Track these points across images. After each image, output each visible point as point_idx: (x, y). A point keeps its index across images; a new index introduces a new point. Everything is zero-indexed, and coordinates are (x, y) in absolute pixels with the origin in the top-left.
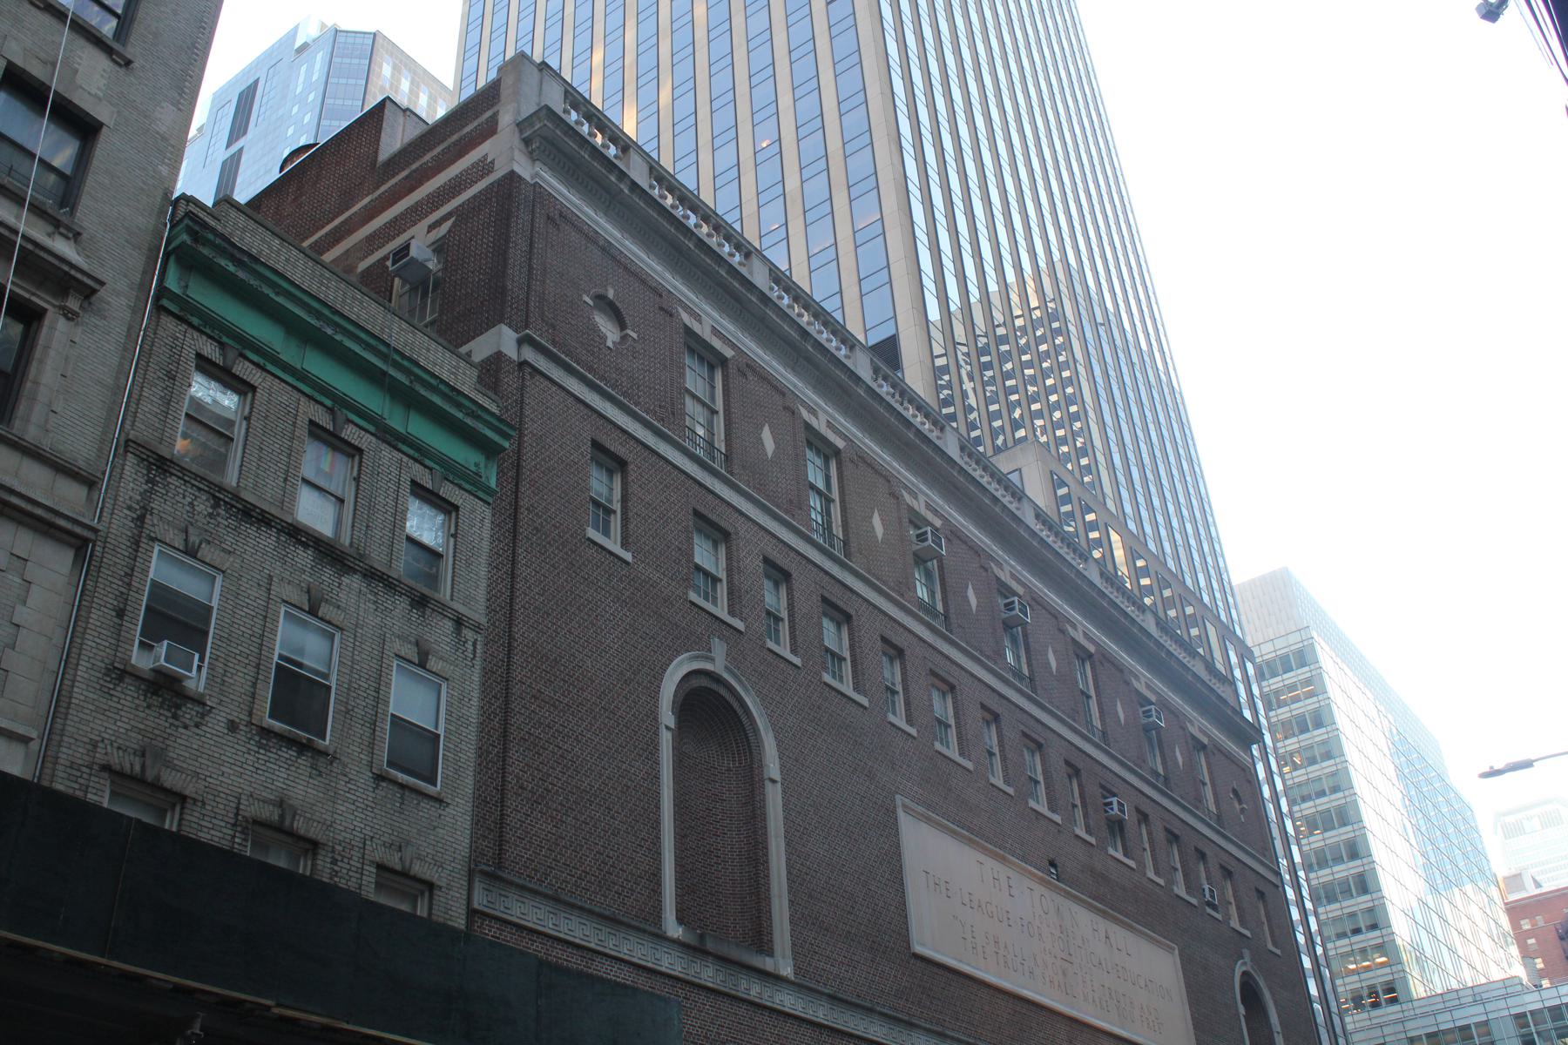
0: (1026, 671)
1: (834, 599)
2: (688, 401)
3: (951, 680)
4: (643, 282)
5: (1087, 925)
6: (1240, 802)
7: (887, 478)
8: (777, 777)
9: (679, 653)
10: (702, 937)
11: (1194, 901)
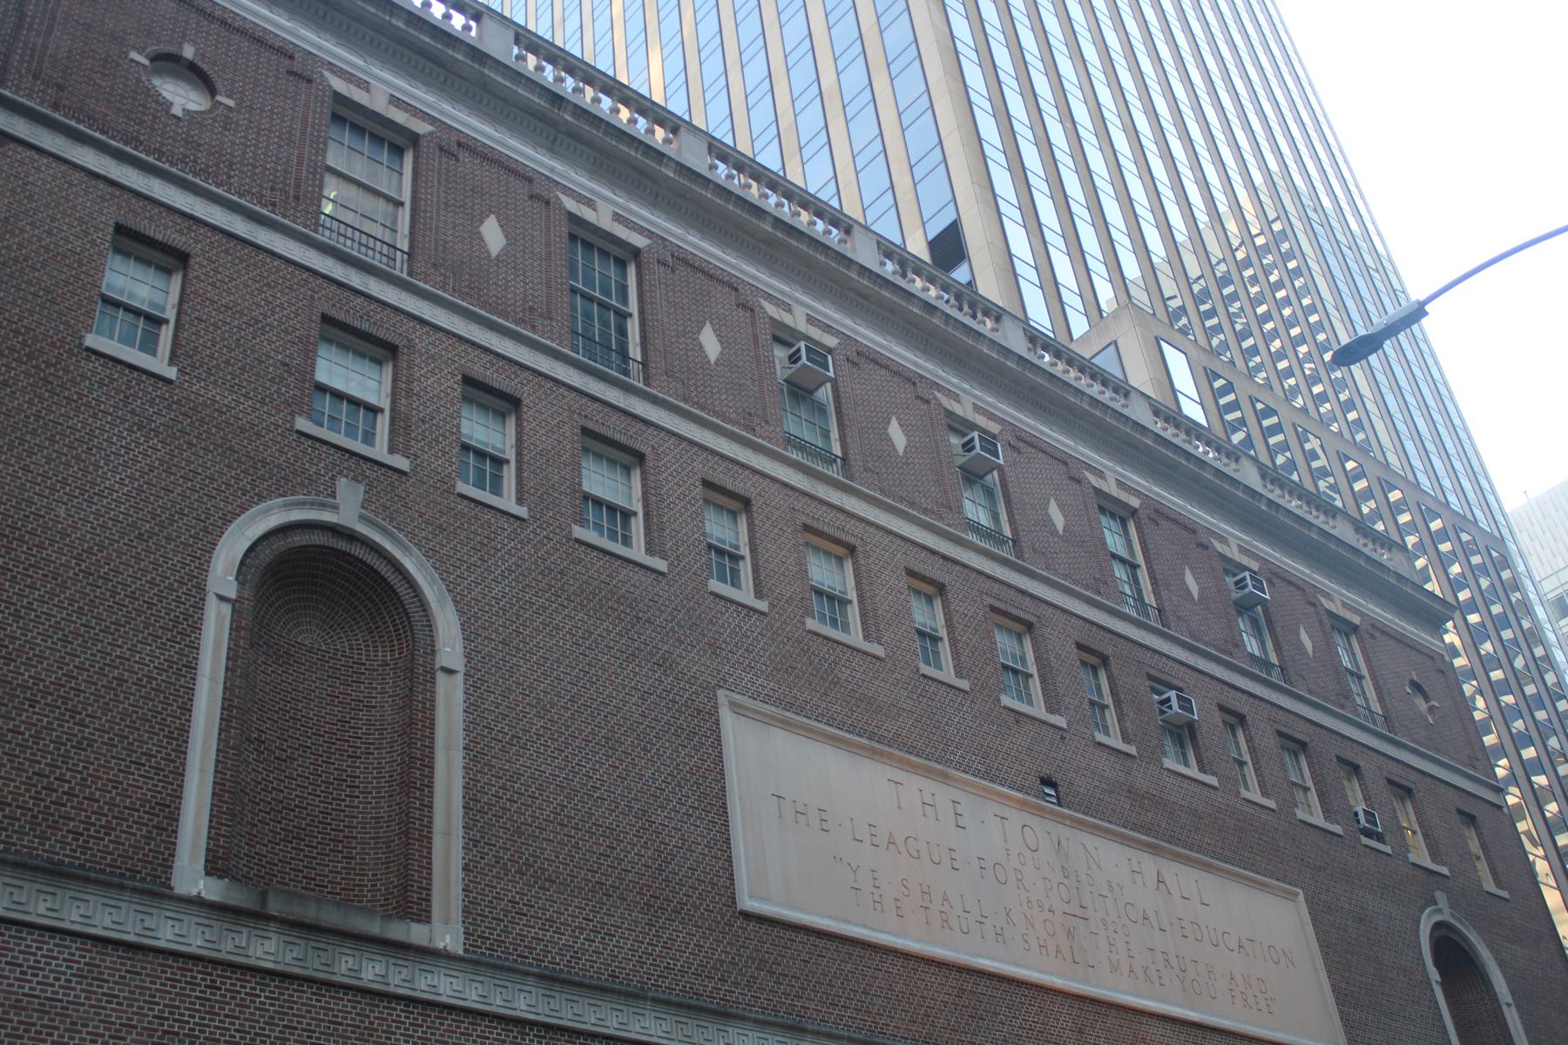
0: (1008, 532)
3: (852, 540)
5: (1116, 865)
6: (1427, 698)
7: (732, 285)
8: (458, 663)
10: (264, 896)
11: (1337, 829)
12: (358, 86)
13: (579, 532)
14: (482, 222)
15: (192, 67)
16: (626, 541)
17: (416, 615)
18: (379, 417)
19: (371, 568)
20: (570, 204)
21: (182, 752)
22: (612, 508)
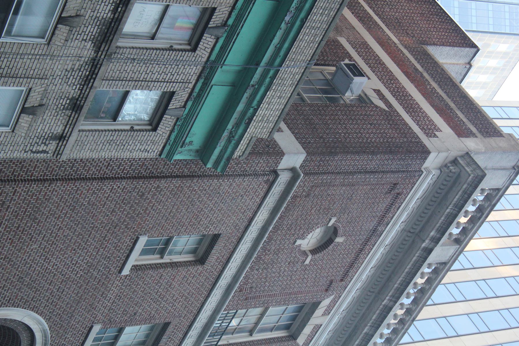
2: (258, 311)
4: (351, 265)
9: (48, 320)
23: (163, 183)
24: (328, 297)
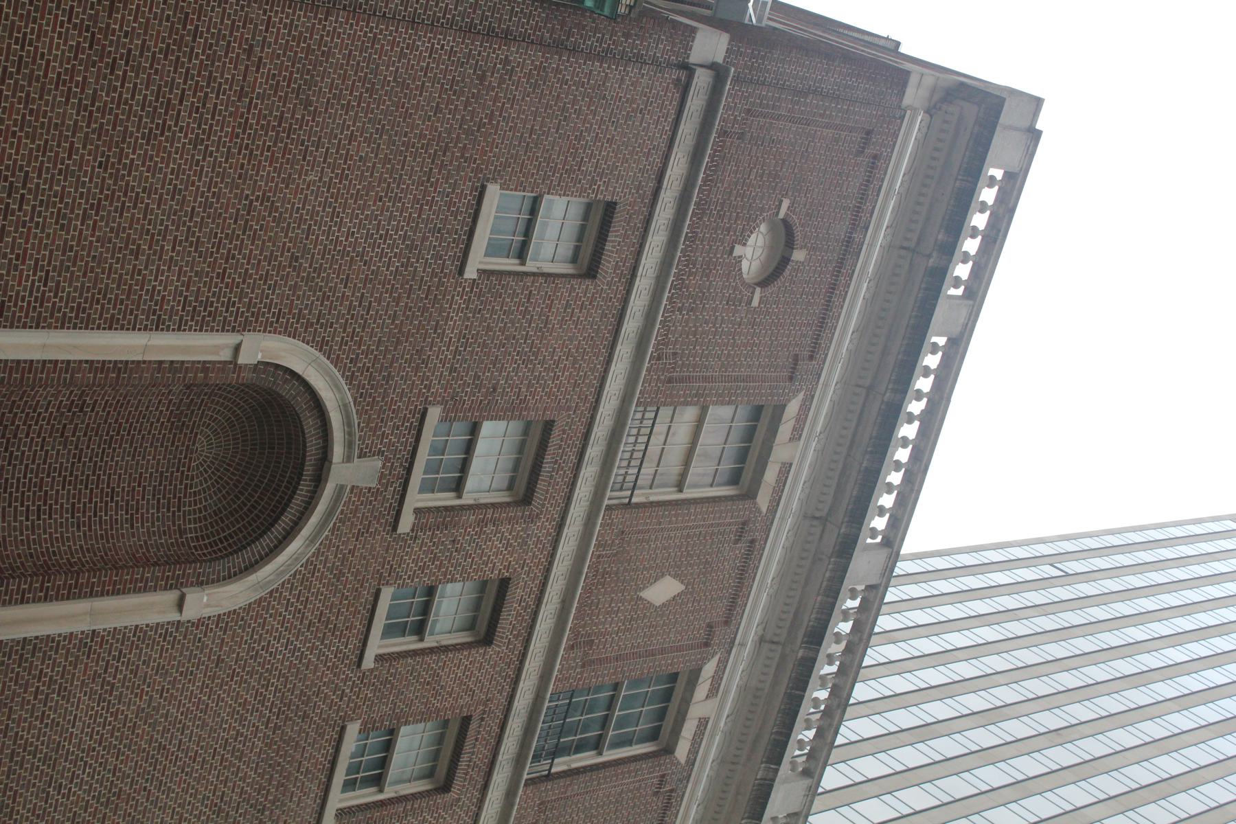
1: (471, 732)
2: (690, 413)
4: (822, 324)
9: (350, 380)
12: (794, 429)
13: (353, 729)
14: (675, 576)
15: (785, 261)
16: (349, 785)
17: (238, 560)
18: (452, 494)
19: (287, 505)
20: (709, 669)
21: (63, 324)
22: (383, 763)
23: (514, 53)
24: (795, 396)
